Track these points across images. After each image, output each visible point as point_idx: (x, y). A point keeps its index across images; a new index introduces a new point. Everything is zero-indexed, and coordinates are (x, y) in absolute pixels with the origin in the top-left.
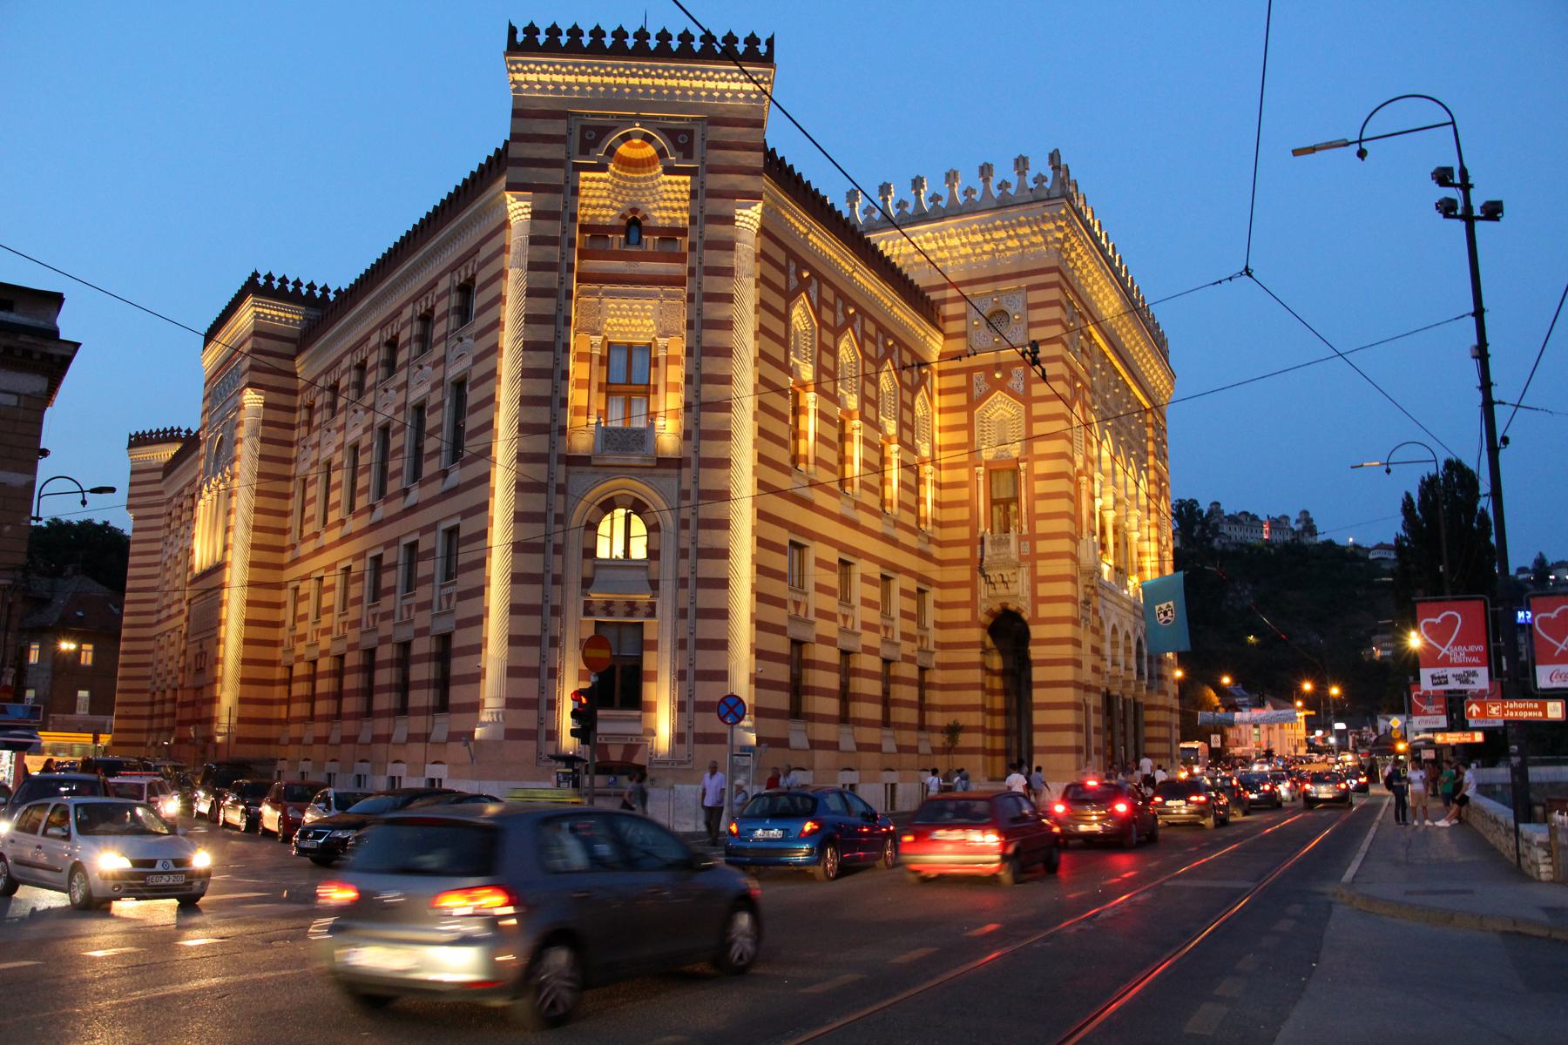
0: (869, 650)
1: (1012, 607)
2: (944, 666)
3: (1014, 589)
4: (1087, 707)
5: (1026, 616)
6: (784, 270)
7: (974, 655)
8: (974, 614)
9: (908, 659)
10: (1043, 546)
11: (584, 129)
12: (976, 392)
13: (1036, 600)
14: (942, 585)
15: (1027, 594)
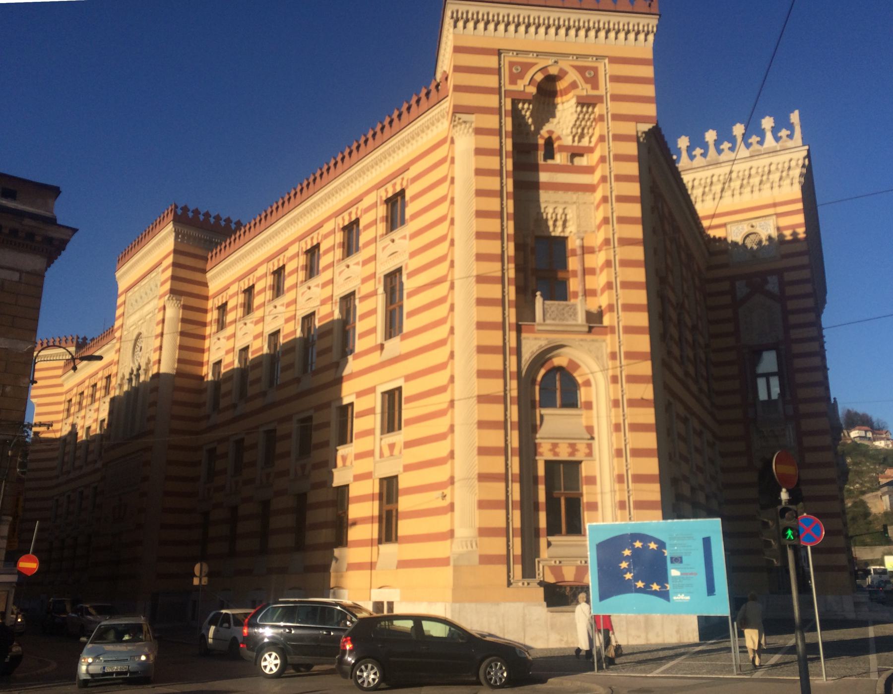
11: (512, 64)
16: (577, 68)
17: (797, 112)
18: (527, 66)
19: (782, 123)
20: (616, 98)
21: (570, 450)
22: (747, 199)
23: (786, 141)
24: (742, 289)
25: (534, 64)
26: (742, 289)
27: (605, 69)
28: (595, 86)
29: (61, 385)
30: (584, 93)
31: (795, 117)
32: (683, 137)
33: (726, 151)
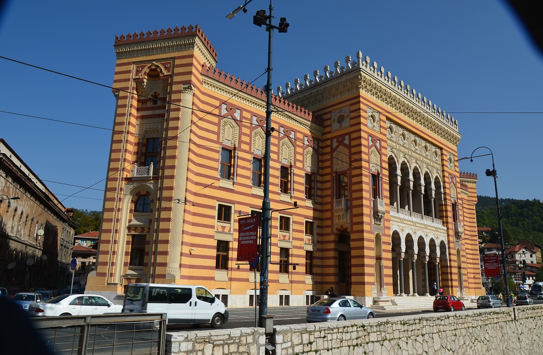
5: (349, 230)
7: (332, 246)
8: (332, 230)
11: (137, 67)
12: (334, 147)
15: (349, 221)
24: (335, 144)
26: (335, 144)
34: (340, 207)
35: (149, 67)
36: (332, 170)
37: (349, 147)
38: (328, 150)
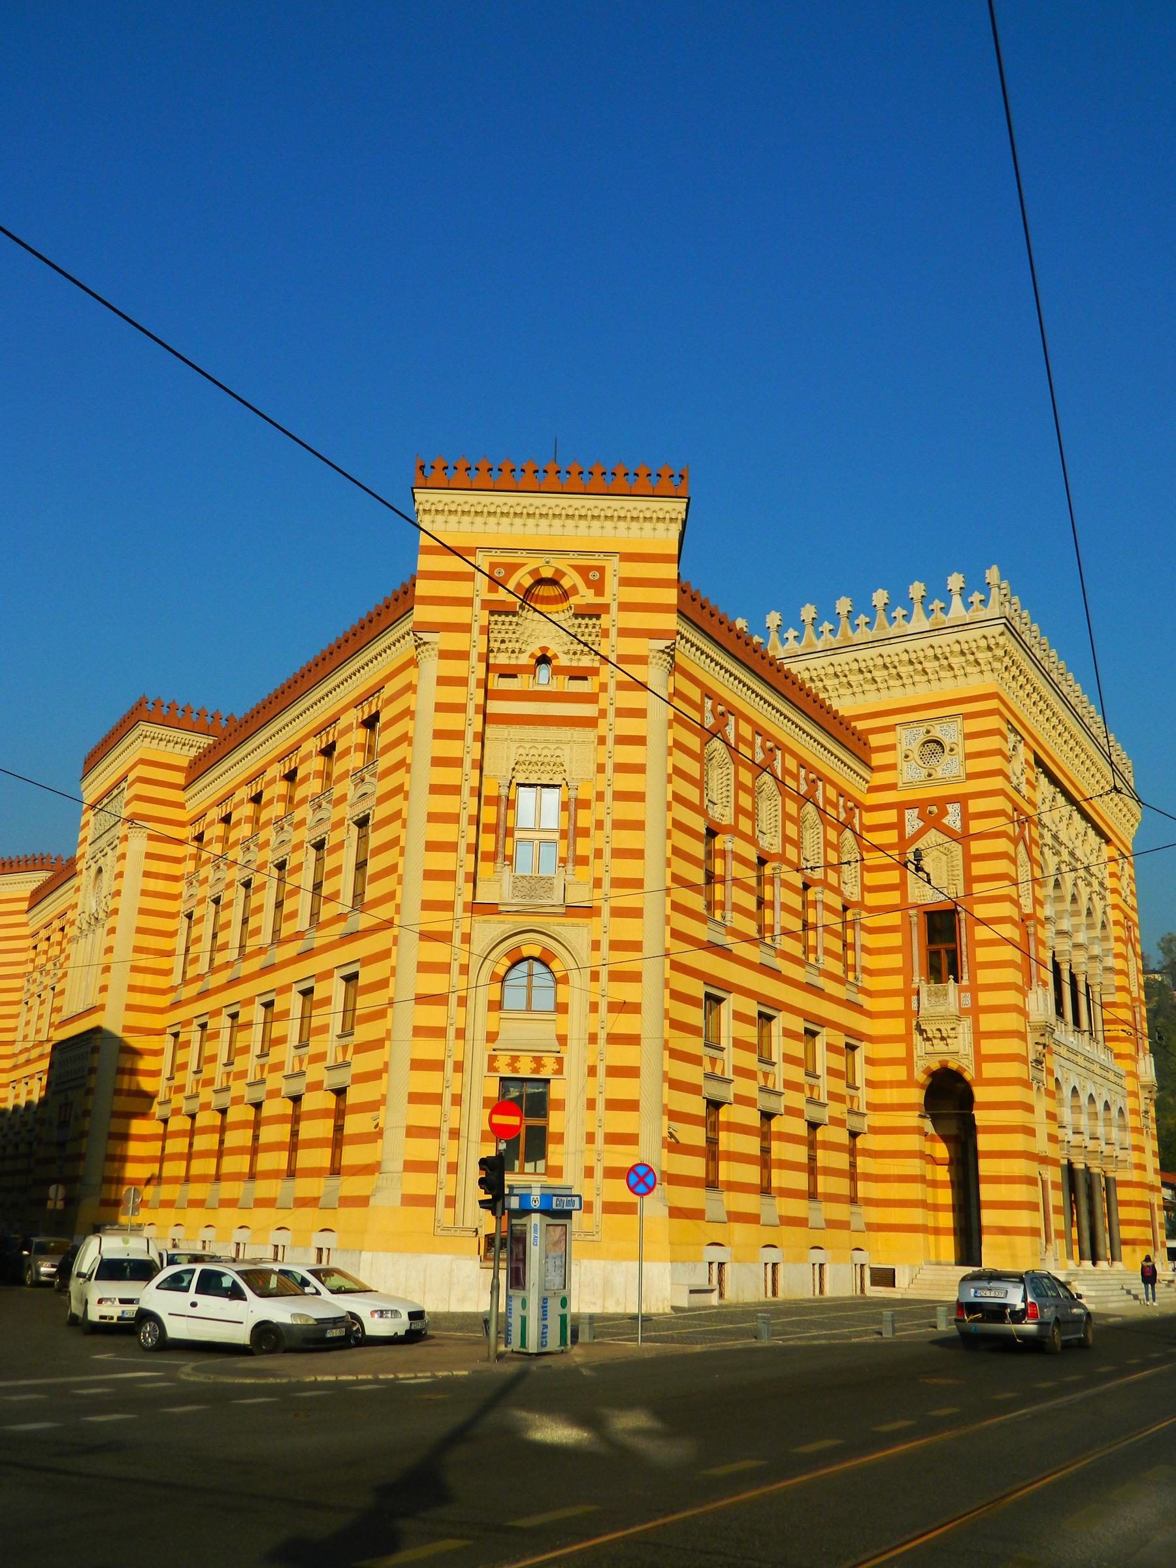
0: (791, 1111)
1: (953, 1065)
2: (874, 1130)
3: (954, 1045)
4: (1044, 1183)
5: (969, 1076)
6: (699, 708)
7: (912, 1119)
9: (837, 1122)
10: (985, 999)
12: (909, 831)
13: (980, 1058)
14: (871, 1039)
15: (970, 1051)
16: (578, 569)
17: (995, 568)
18: (512, 568)
19: (976, 584)
20: (624, 607)
21: (534, 1065)
22: (922, 692)
23: (977, 610)
25: (523, 565)
27: (615, 569)
28: (600, 592)
29: (25, 925)
30: (584, 601)
31: (992, 575)
32: (843, 598)
33: (900, 620)
34: (941, 1009)
35: (535, 572)
36: (904, 896)
37: (964, 838)
38: (891, 837)
